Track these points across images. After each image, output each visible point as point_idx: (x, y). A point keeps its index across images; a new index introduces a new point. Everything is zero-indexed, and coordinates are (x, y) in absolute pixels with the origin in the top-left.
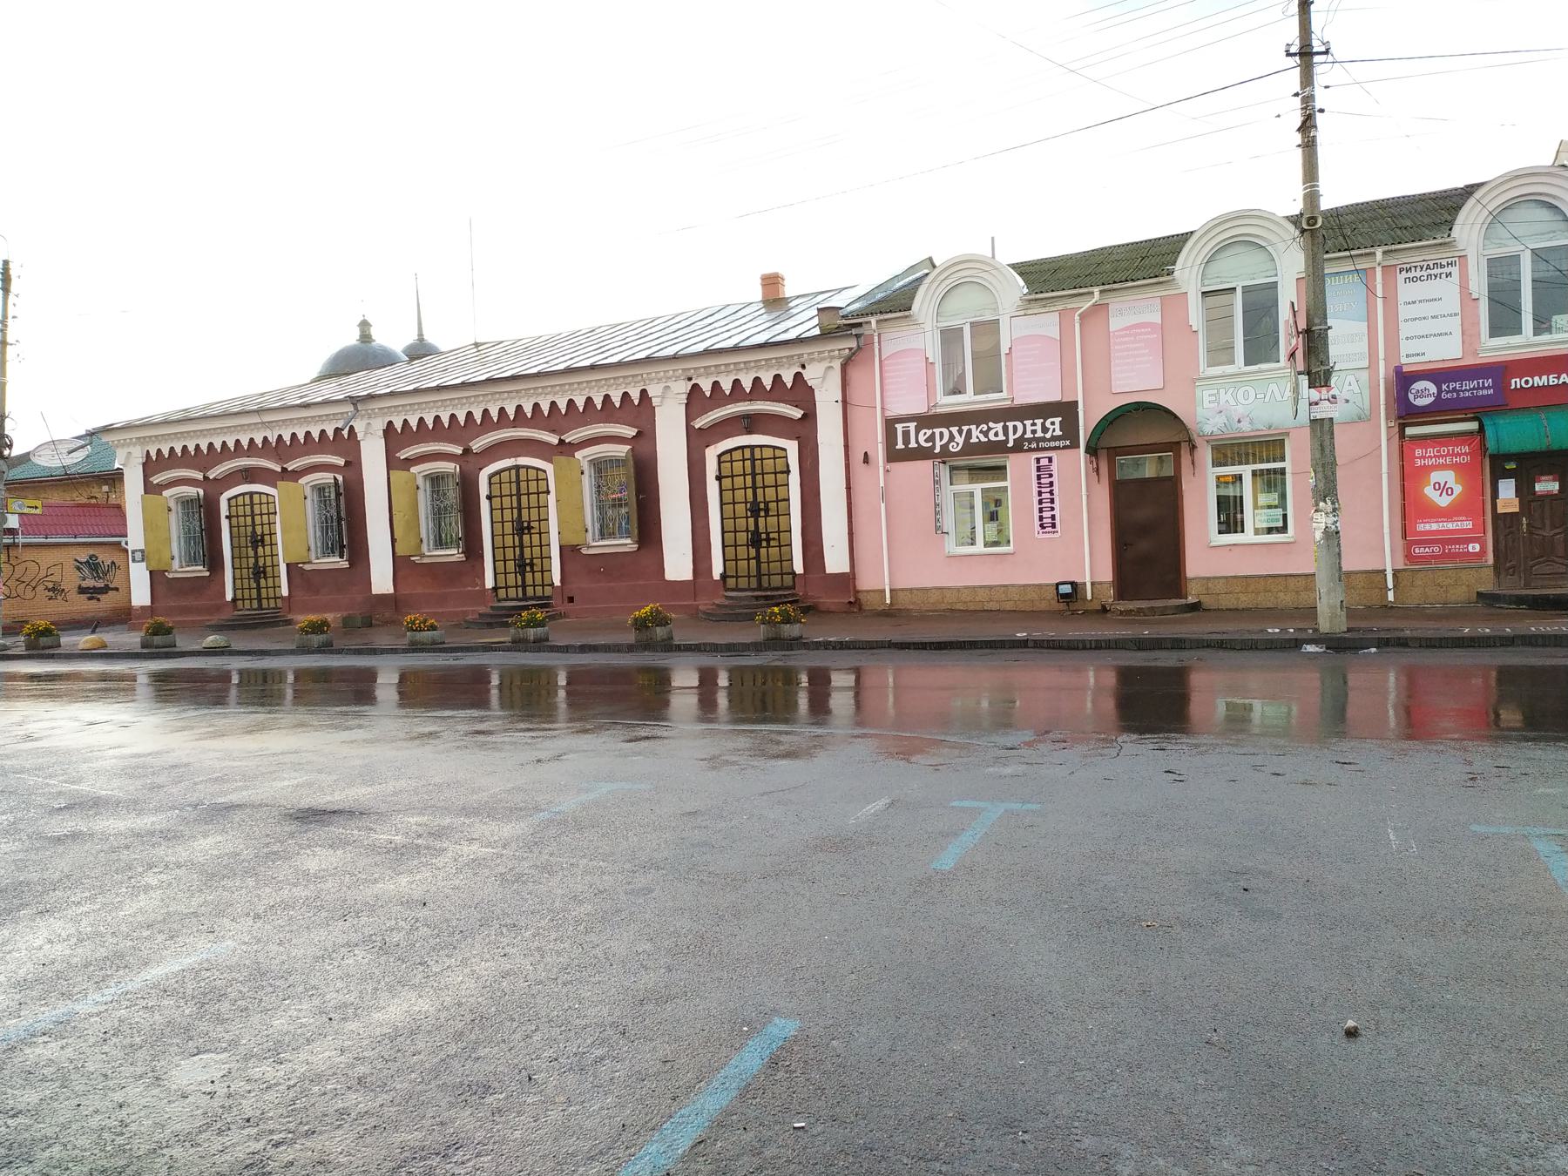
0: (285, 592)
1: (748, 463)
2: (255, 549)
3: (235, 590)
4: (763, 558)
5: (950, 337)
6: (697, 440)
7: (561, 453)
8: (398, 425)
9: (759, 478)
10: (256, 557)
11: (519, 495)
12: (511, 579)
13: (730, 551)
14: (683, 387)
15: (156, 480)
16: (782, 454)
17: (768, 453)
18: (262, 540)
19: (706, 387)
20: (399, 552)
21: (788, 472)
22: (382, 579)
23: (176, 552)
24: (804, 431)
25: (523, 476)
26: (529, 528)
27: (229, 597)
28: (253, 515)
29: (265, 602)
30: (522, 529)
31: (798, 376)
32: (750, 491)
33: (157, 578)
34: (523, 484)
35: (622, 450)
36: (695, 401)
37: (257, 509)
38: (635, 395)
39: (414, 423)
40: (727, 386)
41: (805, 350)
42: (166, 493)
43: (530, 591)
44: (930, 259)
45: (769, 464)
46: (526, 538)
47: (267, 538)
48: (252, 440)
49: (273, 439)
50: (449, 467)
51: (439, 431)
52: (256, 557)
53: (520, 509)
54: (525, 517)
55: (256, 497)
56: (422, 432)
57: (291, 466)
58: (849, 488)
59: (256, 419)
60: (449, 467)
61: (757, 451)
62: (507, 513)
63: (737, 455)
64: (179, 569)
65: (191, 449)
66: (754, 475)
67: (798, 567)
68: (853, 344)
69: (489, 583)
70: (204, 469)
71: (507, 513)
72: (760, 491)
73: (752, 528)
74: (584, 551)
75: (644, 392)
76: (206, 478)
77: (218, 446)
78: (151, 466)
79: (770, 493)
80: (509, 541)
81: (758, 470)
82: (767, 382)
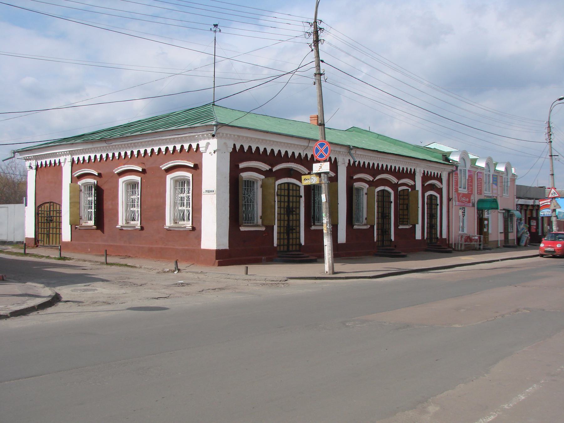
10: (288, 221)
49: (303, 155)
70: (273, 165)
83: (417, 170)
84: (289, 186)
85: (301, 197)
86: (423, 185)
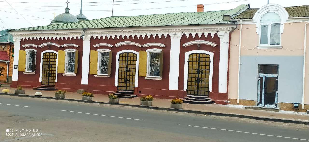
0: (56, 81)
1: (198, 58)
2: (49, 68)
3: (42, 79)
4: (200, 86)
5: (264, 27)
6: (183, 50)
7: (141, 50)
8: (95, 37)
9: (200, 63)
10: (49, 70)
11: (128, 60)
12: (123, 84)
13: (190, 83)
14: (181, 34)
15: (24, 46)
16: (209, 56)
17: (204, 56)
18: (52, 66)
19: (187, 35)
20: (91, 73)
21: (210, 62)
22: (85, 81)
23: (26, 67)
24: (216, 50)
25: (129, 55)
26: (130, 70)
27: (40, 80)
28: (50, 59)
29: (50, 83)
30: (127, 70)
31: (216, 35)
32: (197, 66)
33: (21, 73)
34: (129, 58)
35: (160, 51)
36: (184, 39)
37: (51, 57)
38: (166, 35)
39: (99, 37)
40: (194, 35)
41: (219, 27)
42: (26, 50)
43: (128, 88)
44: (249, 5)
45: (204, 59)
46: (128, 73)
47: (53, 65)
48: (52, 38)
49: (58, 38)
50: (109, 51)
51: (106, 40)
52: (49, 70)
53: (127, 64)
54: (129, 67)
55: (51, 54)
56: (101, 40)
57: (62, 46)
58: (228, 68)
59: (55, 32)
60: (109, 51)
61: (201, 55)
62: (124, 65)
63: (195, 55)
64: (27, 71)
65: (35, 38)
66: (199, 62)
67: (210, 90)
68: (234, 27)
69: (116, 85)
70: (38, 44)
71: (124, 65)
72: (200, 67)
73: (197, 77)
74: (145, 78)
75: (168, 35)
76: (38, 47)
77: (42, 38)
78: (23, 42)
79: (204, 67)
80: (123, 73)
81: (201, 60)
82: (206, 35)
83: (171, 35)
84: (50, 54)
85: (42, 58)
86: (181, 47)
